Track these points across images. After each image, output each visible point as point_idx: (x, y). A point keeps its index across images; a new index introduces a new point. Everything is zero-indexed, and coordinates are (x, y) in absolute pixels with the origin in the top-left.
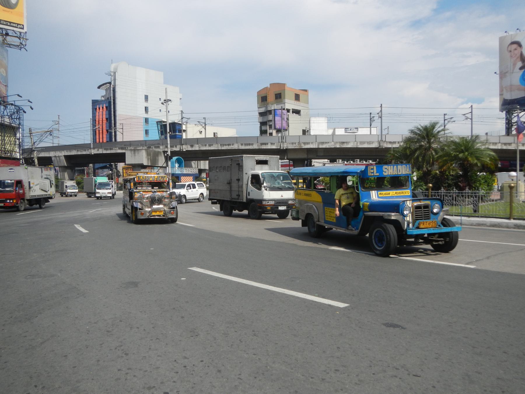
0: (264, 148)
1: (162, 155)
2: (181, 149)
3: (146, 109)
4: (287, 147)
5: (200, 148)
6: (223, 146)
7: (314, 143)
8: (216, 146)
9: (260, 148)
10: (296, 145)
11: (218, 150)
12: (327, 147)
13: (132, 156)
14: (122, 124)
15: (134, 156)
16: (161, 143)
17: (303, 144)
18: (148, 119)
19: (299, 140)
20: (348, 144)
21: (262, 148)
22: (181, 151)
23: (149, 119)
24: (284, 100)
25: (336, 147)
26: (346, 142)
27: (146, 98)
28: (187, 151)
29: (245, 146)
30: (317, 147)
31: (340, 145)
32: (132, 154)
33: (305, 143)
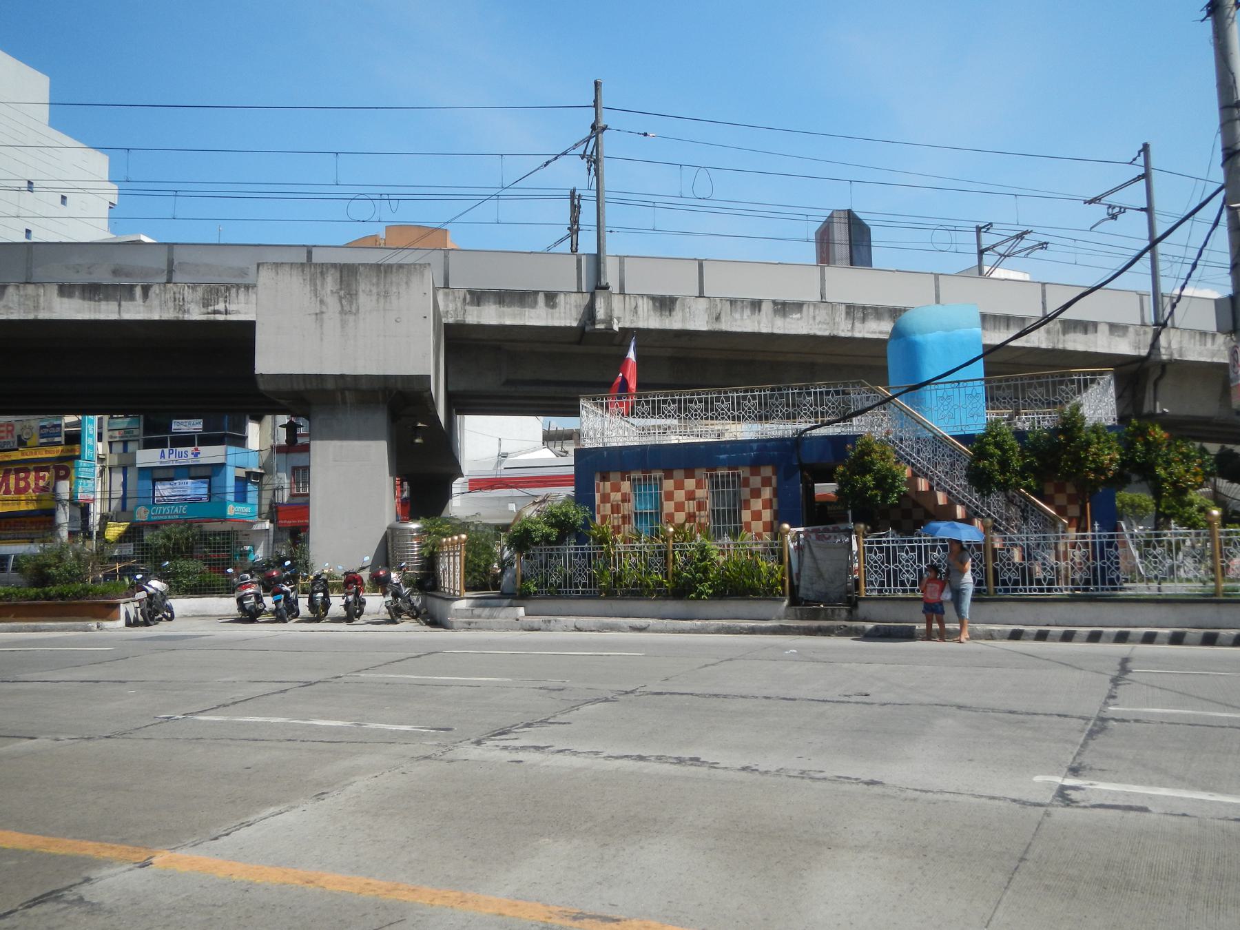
0: (1081, 348)
2: (600, 313)
5: (718, 318)
6: (864, 320)
8: (822, 314)
9: (1060, 346)
11: (833, 339)
13: (319, 315)
15: (342, 312)
21: (1070, 346)
22: (600, 326)
32: (322, 302)
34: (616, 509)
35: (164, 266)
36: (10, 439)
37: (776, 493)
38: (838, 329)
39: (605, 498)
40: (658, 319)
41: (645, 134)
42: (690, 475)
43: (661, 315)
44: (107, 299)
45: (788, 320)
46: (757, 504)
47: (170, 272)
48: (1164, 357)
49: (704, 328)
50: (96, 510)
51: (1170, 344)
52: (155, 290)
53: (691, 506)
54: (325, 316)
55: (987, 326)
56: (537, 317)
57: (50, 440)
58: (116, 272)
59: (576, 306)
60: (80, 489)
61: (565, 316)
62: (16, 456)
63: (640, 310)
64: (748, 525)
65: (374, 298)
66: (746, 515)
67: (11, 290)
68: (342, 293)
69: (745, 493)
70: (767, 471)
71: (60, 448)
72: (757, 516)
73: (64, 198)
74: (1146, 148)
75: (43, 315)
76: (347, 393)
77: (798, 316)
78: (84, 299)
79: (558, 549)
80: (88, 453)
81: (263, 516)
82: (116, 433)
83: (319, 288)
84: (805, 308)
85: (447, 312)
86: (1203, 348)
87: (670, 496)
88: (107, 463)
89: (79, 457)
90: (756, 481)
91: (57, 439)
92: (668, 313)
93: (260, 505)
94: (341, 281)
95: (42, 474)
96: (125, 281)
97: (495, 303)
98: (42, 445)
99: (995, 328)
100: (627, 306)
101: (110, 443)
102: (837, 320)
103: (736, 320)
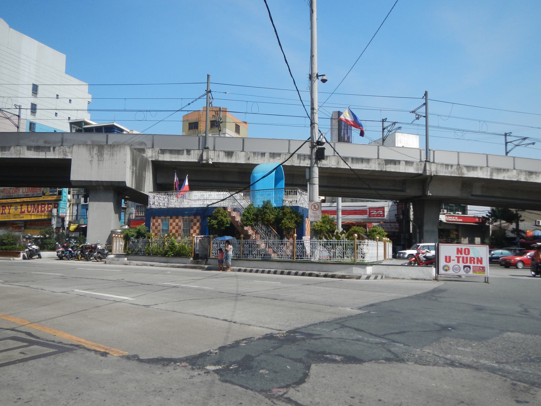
0: (393, 170)
1: (150, 171)
2: (205, 157)
3: (34, 108)
4: (436, 173)
5: (249, 159)
6: (304, 160)
7: (485, 169)
9: (384, 170)
10: (453, 170)
12: (506, 179)
13: (91, 161)
14: (19, 106)
15: (99, 160)
16: (149, 144)
17: (465, 168)
18: (35, 124)
19: (458, 162)
20: (538, 176)
21: (388, 170)
22: (204, 162)
23: (37, 125)
24: (224, 129)
25: (519, 180)
26: (536, 173)
27: (35, 89)
28: (216, 165)
29: (352, 163)
30: (489, 177)
31: (526, 177)
32: (92, 157)
33: (468, 168)
34: (156, 228)
35: (60, 140)
36: (40, 193)
37: (201, 224)
38: (294, 163)
39: (154, 224)
40: (227, 159)
41: (226, 93)
42: (177, 218)
43: (228, 158)
44: (42, 151)
45: (275, 160)
46: (195, 228)
47: (62, 142)
48: (428, 174)
49: (244, 163)
50: (67, 219)
51: (431, 168)
52: (57, 148)
53: (177, 228)
54: (93, 162)
55: (354, 162)
56: (183, 158)
57: (53, 193)
58: (45, 142)
59: (197, 155)
60: (61, 212)
61: (193, 158)
62: (41, 199)
63: (220, 156)
64: (192, 234)
65: (109, 156)
66: (192, 231)
67: (12, 148)
68: (99, 154)
69: (192, 224)
70: (198, 217)
71: (56, 196)
72: (195, 232)
73: (70, 100)
74: (426, 94)
75: (22, 156)
76: (100, 187)
77: (279, 158)
78: (34, 151)
79: (247, 241)
80: (64, 199)
81: (126, 223)
82: (75, 192)
83: (92, 152)
84: (282, 155)
85: (152, 156)
86: (447, 170)
87: (171, 224)
88: (72, 202)
89: (61, 200)
90: (195, 220)
91: (55, 193)
92: (230, 157)
93: (125, 219)
94: (99, 151)
95: (50, 206)
96: (47, 145)
97: (169, 153)
98: (51, 195)
99: (357, 163)
100: (216, 155)
101: (73, 195)
102: (294, 160)
103: (255, 160)
